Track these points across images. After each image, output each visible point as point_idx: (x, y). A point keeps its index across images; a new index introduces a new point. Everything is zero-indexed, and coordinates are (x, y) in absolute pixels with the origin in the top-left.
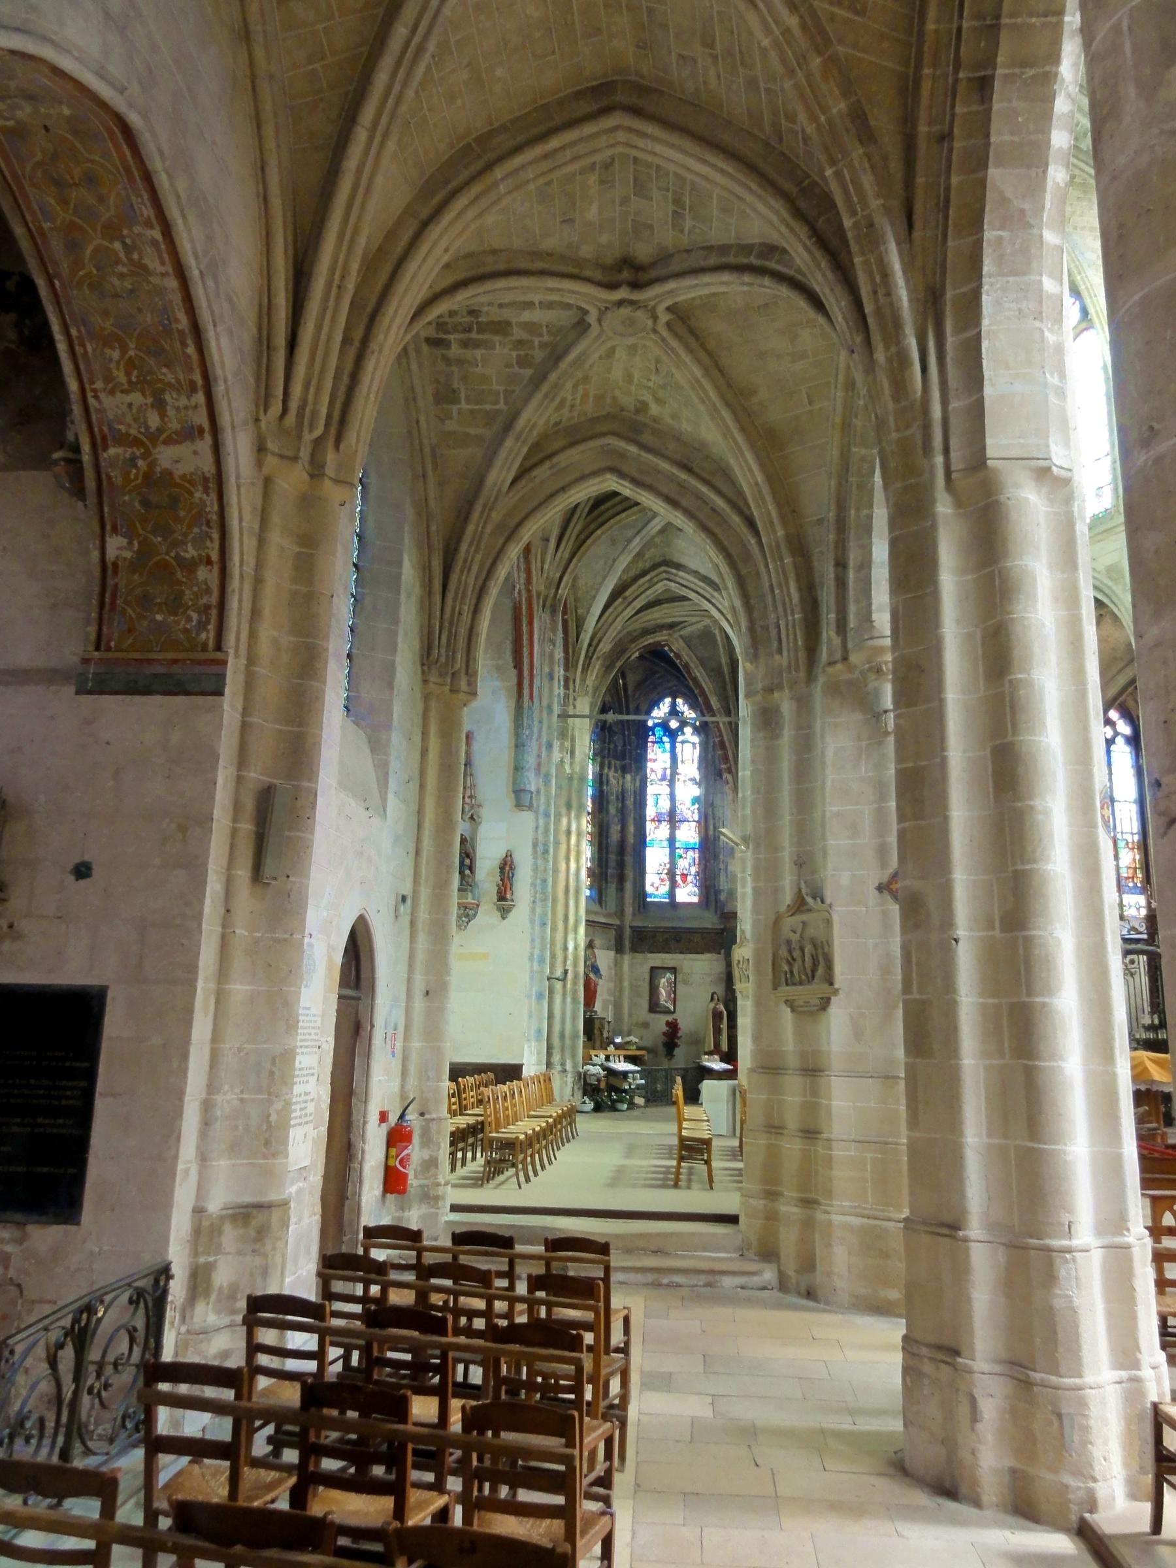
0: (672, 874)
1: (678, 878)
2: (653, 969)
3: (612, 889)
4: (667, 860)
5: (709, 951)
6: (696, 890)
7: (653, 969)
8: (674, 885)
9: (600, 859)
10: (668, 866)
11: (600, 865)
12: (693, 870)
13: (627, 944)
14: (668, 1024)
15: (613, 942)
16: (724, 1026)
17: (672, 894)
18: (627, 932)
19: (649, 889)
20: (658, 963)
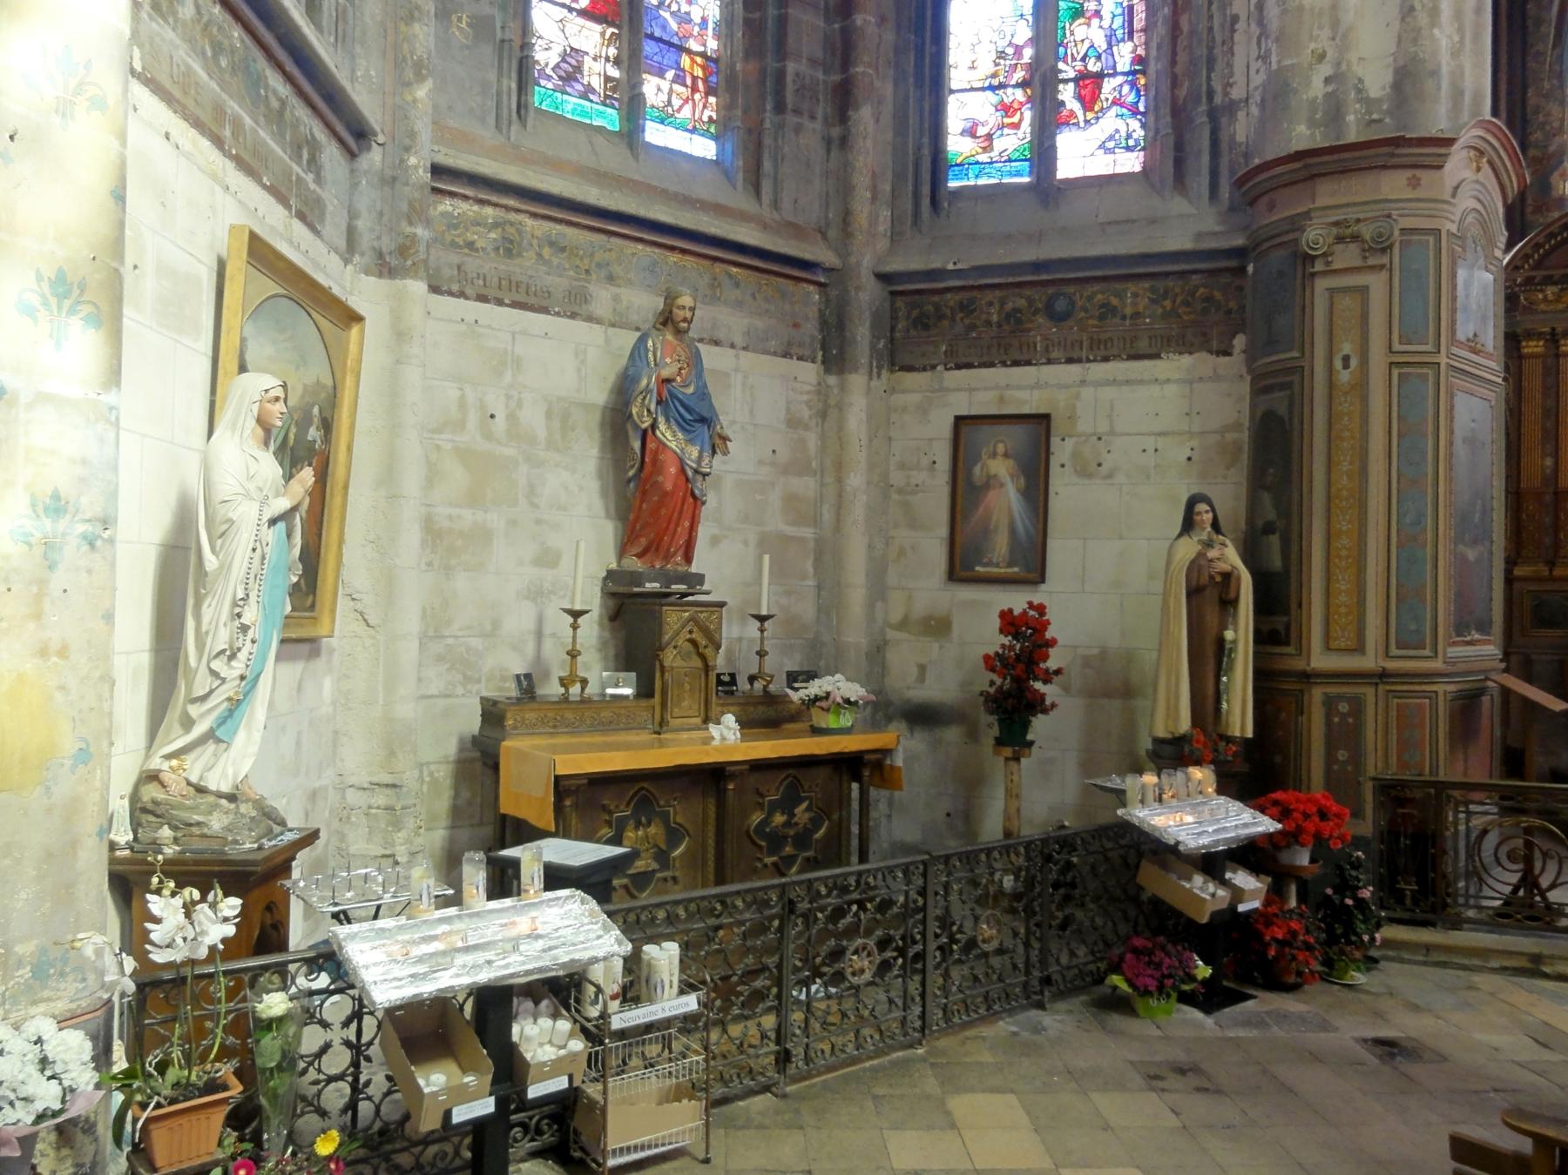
0: (1041, 82)
1: (1067, 93)
2: (959, 420)
3: (809, 136)
4: (1024, 33)
5: (1185, 347)
6: (1135, 124)
7: (959, 420)
8: (1049, 120)
9: (754, 28)
10: (1028, 53)
11: (754, 48)
12: (1124, 56)
13: (862, 333)
14: (1010, 623)
15: (811, 328)
16: (1241, 632)
17: (1042, 153)
18: (866, 295)
19: (957, 145)
20: (983, 404)
